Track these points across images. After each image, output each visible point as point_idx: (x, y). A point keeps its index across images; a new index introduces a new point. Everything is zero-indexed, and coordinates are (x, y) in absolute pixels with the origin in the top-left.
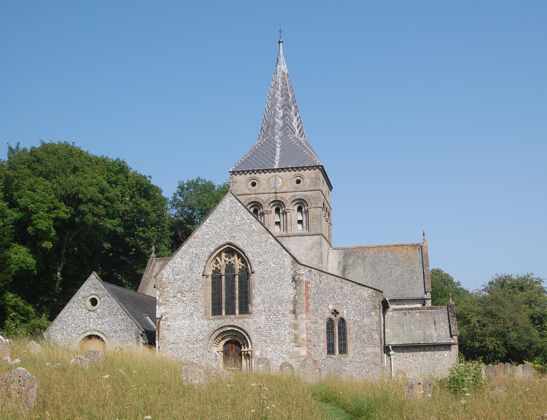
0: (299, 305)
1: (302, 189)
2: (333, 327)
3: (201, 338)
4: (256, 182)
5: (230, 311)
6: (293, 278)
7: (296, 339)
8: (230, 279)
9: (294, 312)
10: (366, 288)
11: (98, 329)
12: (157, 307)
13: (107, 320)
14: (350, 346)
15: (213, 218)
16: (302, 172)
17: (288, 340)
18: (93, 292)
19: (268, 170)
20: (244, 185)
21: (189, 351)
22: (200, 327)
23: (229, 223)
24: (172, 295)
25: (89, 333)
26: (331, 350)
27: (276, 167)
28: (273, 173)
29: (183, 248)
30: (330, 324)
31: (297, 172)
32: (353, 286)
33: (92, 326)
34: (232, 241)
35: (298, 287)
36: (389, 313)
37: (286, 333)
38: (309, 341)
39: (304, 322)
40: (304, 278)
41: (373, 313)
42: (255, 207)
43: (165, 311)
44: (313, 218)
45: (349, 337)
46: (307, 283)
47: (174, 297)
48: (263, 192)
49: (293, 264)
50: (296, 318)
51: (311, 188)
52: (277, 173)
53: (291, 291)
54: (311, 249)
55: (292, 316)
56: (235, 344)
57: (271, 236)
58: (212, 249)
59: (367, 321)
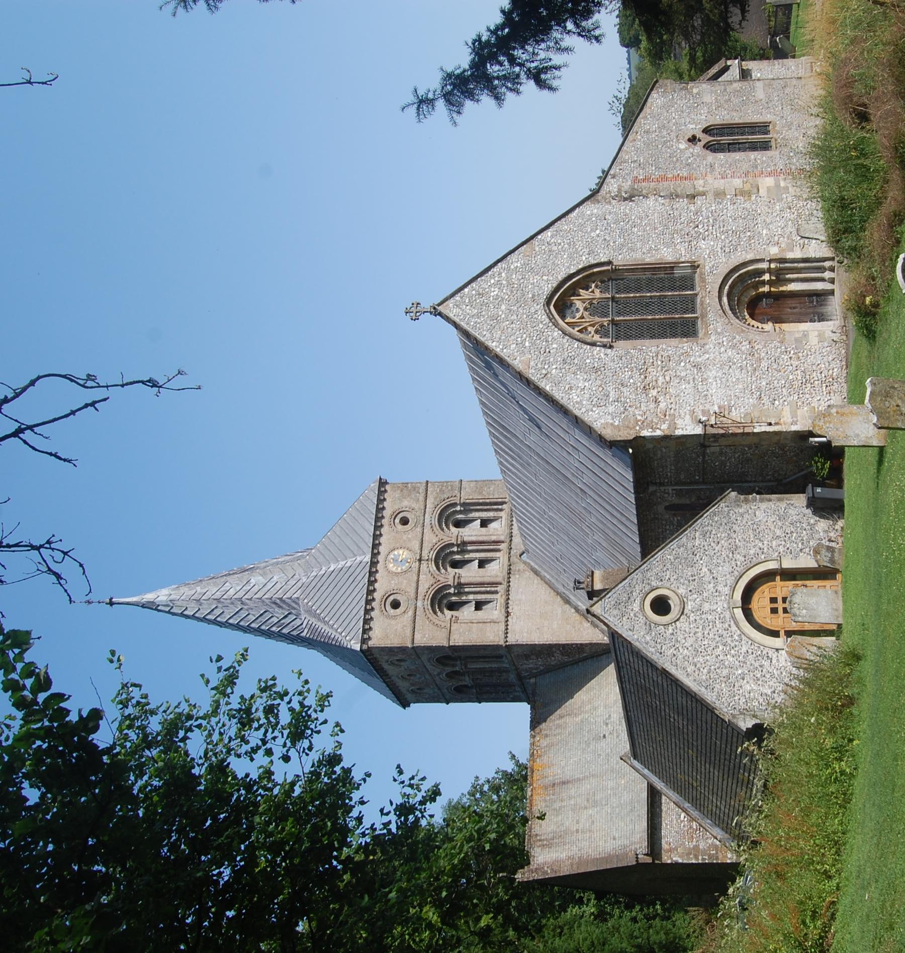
0: (679, 190)
1: (420, 513)
3: (745, 347)
4: (392, 598)
5: (690, 304)
6: (625, 199)
8: (622, 306)
9: (693, 197)
10: (650, 100)
11: (726, 590)
12: (679, 432)
13: (705, 569)
15: (488, 335)
16: (387, 513)
17: (747, 205)
18: (636, 606)
19: (371, 573)
20: (393, 622)
21: (775, 366)
22: (723, 349)
23: (503, 307)
24: (652, 405)
25: (739, 613)
26: (765, 146)
28: (379, 567)
29: (548, 388)
32: (645, 118)
33: (721, 605)
34: (542, 300)
35: (644, 192)
38: (746, 174)
39: (710, 182)
40: (627, 185)
41: (695, 91)
43: (688, 417)
44: (480, 493)
47: (656, 401)
48: (414, 585)
49: (599, 202)
50: (703, 194)
51: (421, 498)
52: (380, 558)
53: (651, 202)
55: (699, 201)
57: (539, 237)
58: (556, 334)
59: (708, 98)
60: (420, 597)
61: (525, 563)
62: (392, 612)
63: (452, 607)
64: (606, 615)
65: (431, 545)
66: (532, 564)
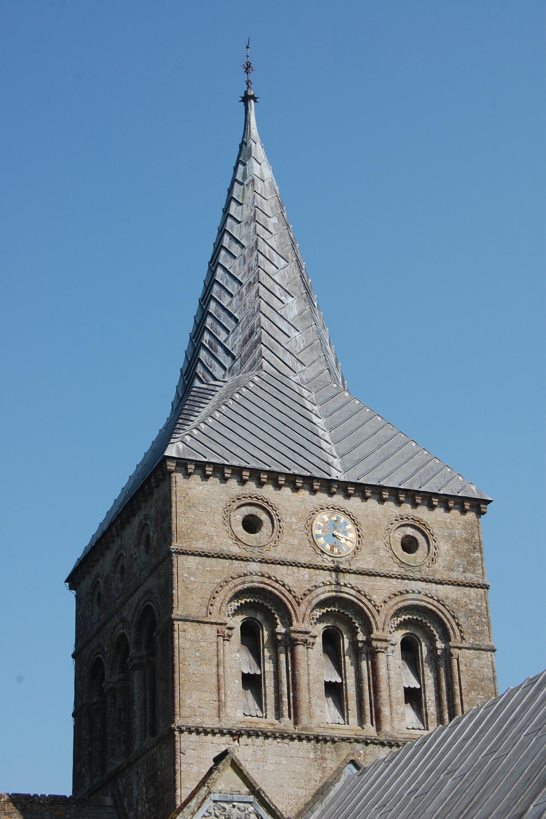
4: (264, 517)
20: (218, 518)
28: (322, 498)
31: (407, 509)
42: (252, 614)
48: (290, 558)
51: (455, 576)
52: (338, 499)
60: (265, 568)
61: (339, 771)
62: (238, 516)
63: (250, 635)
64: (208, 804)
65: (367, 590)
66: (338, 786)
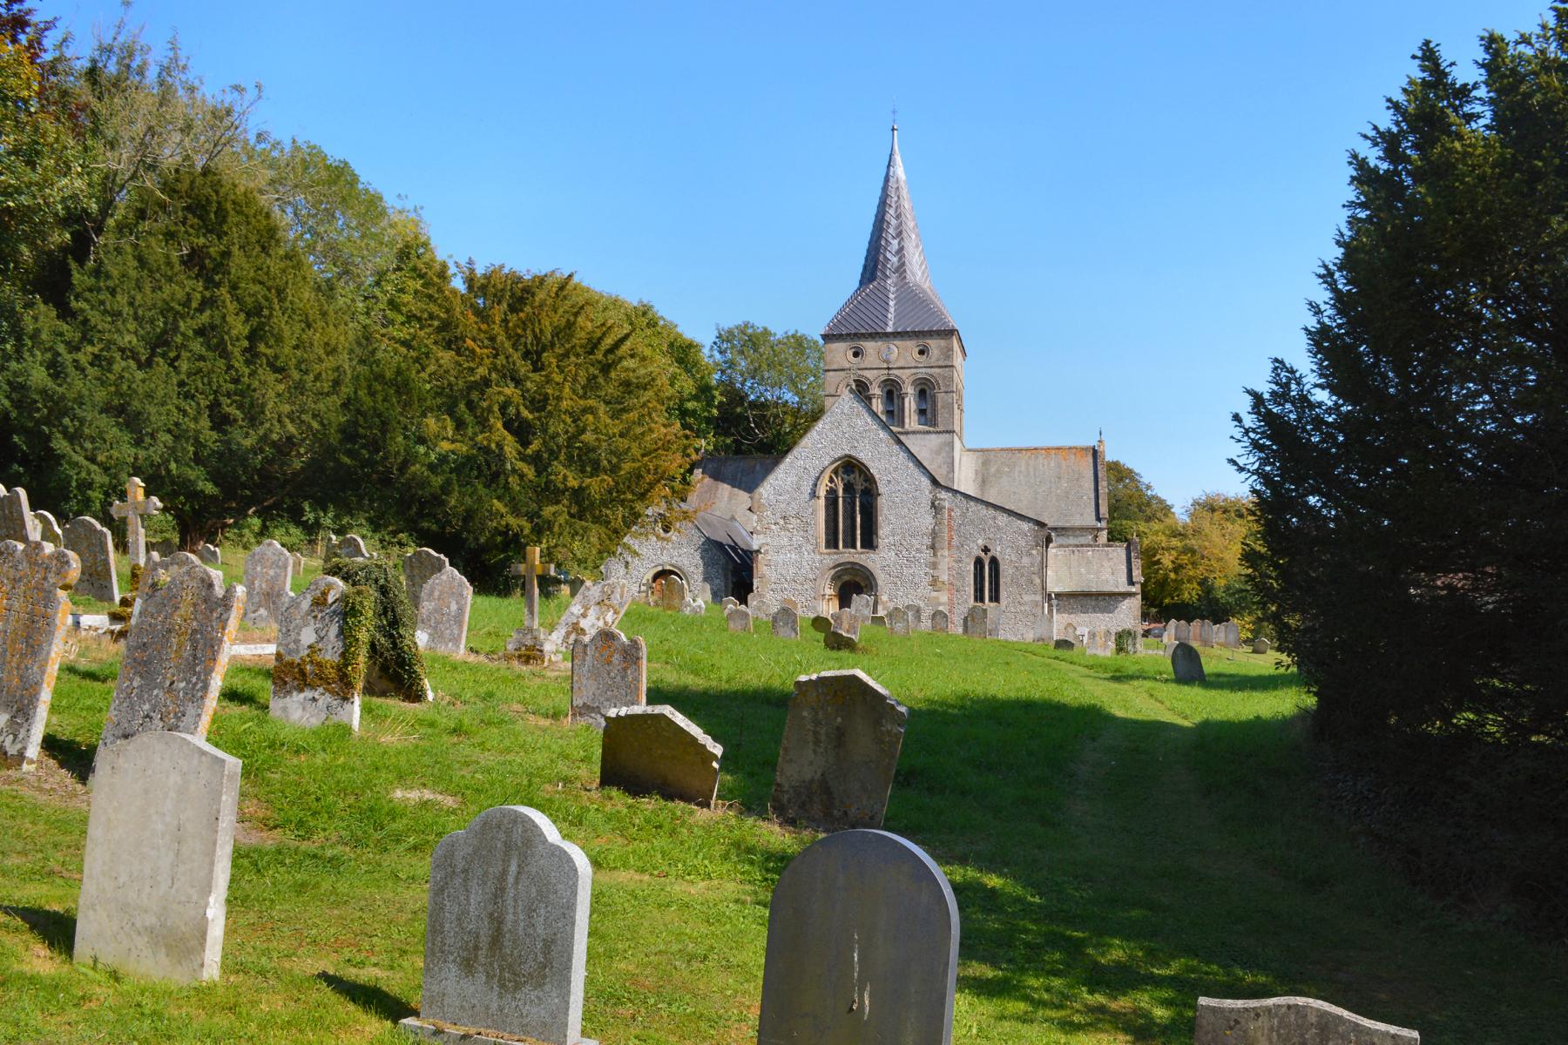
2: (982, 568)
7: (934, 582)
9: (933, 547)
14: (1003, 594)
17: (925, 583)
27: (889, 330)
30: (979, 563)
33: (665, 558)
36: (1052, 550)
37: (921, 573)
40: (947, 504)
45: (1002, 581)
46: (950, 510)
50: (935, 555)
54: (938, 453)
56: (853, 584)
59: (1026, 561)
62: (850, 353)
